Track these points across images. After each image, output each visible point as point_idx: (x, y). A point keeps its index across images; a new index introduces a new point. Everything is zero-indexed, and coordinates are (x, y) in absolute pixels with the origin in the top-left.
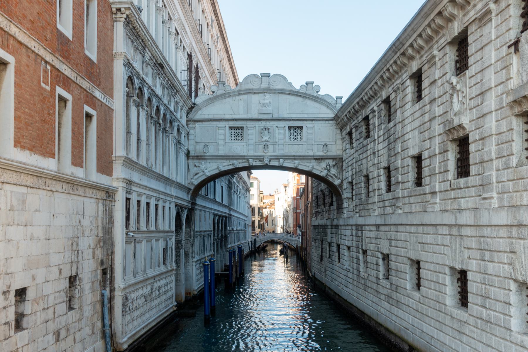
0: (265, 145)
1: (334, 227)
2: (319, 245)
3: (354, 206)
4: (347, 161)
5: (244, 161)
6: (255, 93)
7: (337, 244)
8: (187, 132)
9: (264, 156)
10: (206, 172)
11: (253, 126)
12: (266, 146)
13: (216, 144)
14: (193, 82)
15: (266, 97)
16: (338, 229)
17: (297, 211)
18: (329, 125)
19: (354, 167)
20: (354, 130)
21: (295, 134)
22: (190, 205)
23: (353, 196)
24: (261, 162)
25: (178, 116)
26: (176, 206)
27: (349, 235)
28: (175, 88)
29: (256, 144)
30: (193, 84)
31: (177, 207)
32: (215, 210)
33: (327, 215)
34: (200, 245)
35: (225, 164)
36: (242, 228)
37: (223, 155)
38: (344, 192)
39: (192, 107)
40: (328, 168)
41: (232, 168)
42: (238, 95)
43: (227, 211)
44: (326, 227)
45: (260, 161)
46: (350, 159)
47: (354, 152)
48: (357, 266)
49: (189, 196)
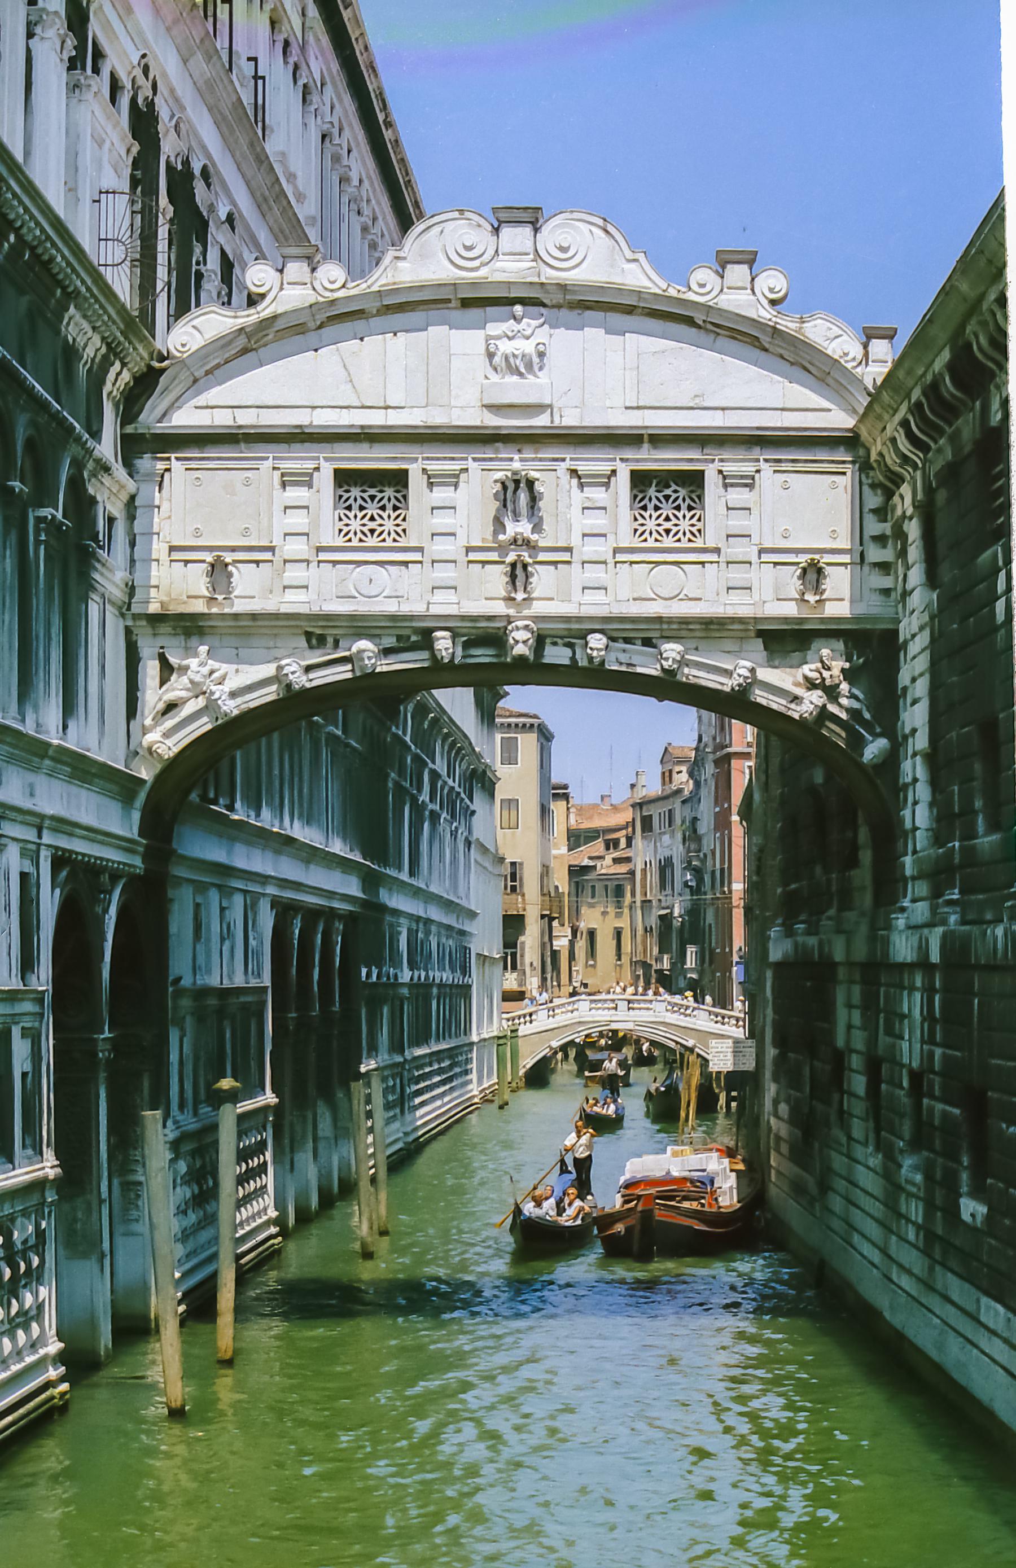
0: (513, 565)
6: (466, 303)
8: (124, 497)
9: (509, 619)
10: (220, 692)
11: (456, 466)
12: (519, 566)
13: (267, 556)
14: (162, 245)
15: (520, 327)
22: (138, 861)
24: (491, 652)
26: (61, 860)
29: (473, 556)
30: (162, 259)
31: (64, 874)
32: (284, 883)
34: (196, 1059)
36: (446, 976)
37: (304, 609)
39: (150, 367)
41: (349, 675)
43: (352, 887)
49: (136, 816)
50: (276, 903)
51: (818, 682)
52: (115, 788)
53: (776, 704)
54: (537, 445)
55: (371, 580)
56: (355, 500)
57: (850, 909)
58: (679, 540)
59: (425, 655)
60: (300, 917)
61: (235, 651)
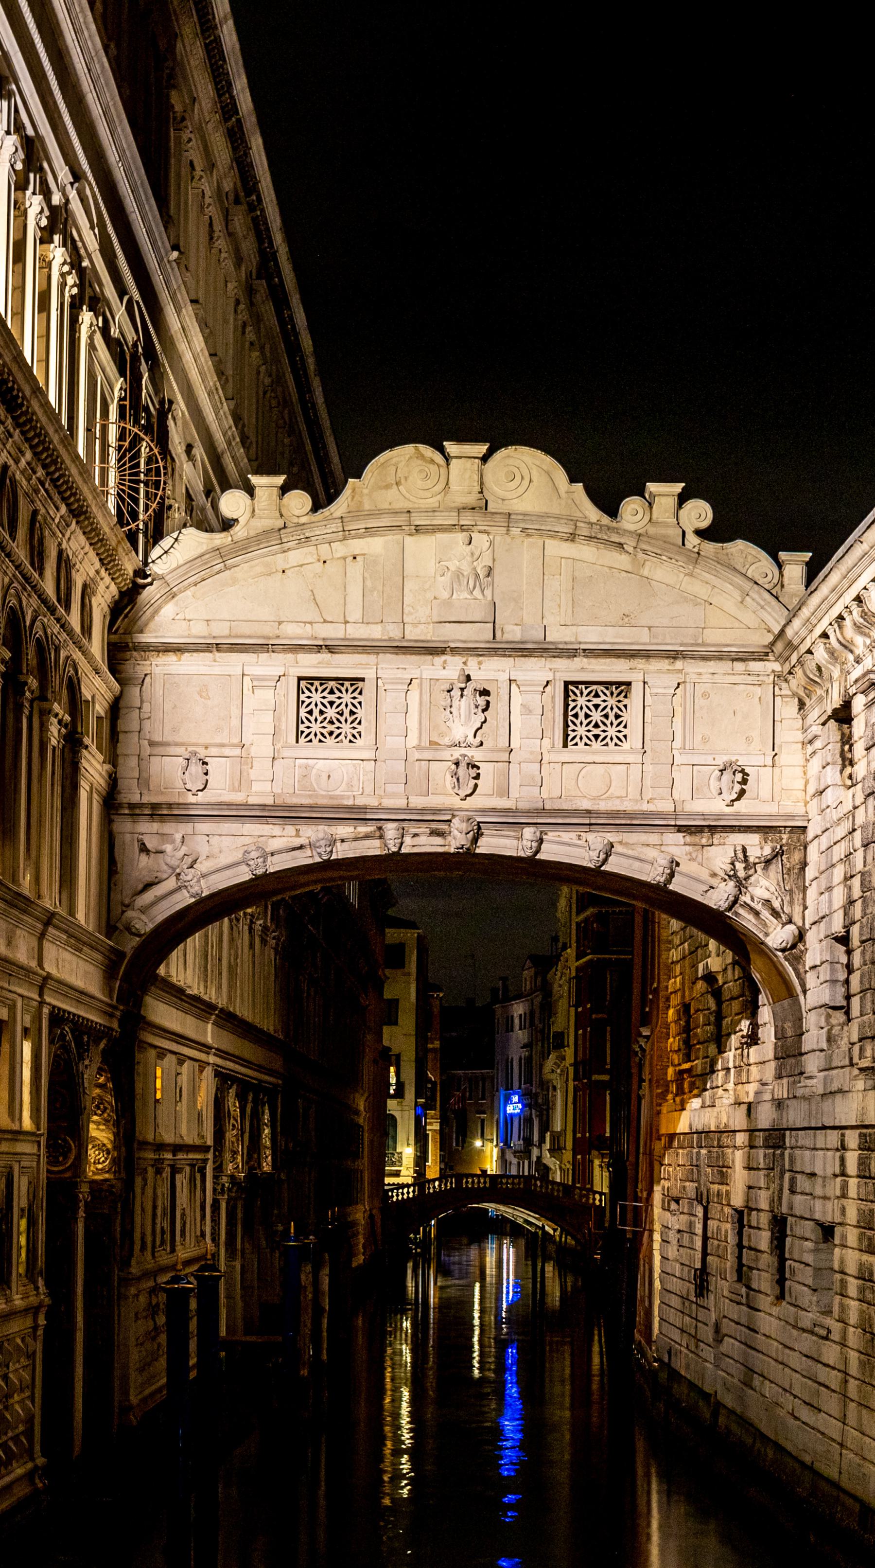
1: (760, 1140)
2: (691, 1224)
3: (853, 1044)
4: (824, 841)
5: (363, 829)
7: (774, 1217)
9: (453, 814)
12: (463, 765)
16: (783, 1147)
17: (595, 1077)
18: (750, 679)
19: (859, 866)
20: (859, 703)
21: (596, 716)
23: (848, 997)
24: (438, 840)
25: (74, 620)
27: (829, 1172)
28: (64, 499)
33: (730, 1086)
34: (155, 1207)
35: (275, 844)
38: (811, 980)
40: (741, 874)
41: (310, 861)
42: (345, 539)
44: (726, 1140)
45: (435, 833)
46: (841, 831)
47: (860, 799)
48: (862, 1312)
50: (217, 1074)
51: (732, 873)
52: (99, 957)
53: (694, 892)
54: (481, 658)
55: (329, 776)
56: (316, 705)
57: (748, 1083)
58: (607, 745)
59: (377, 843)
60: (235, 1087)
61: (207, 838)
